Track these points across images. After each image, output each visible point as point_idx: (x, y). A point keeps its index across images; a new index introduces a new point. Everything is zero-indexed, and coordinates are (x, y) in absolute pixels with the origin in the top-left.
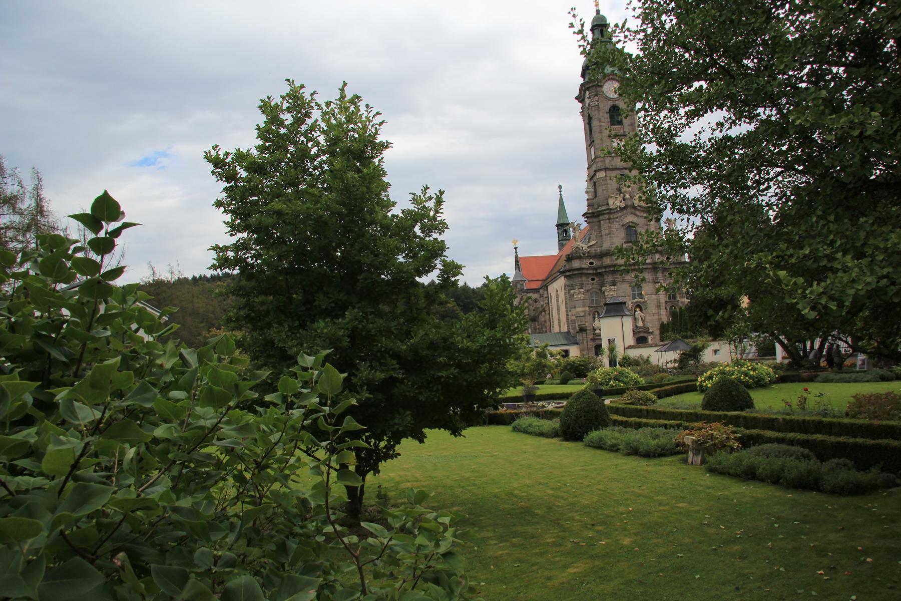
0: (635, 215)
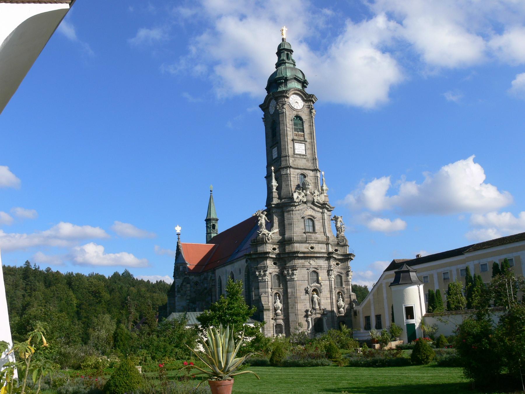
0: (314, 209)
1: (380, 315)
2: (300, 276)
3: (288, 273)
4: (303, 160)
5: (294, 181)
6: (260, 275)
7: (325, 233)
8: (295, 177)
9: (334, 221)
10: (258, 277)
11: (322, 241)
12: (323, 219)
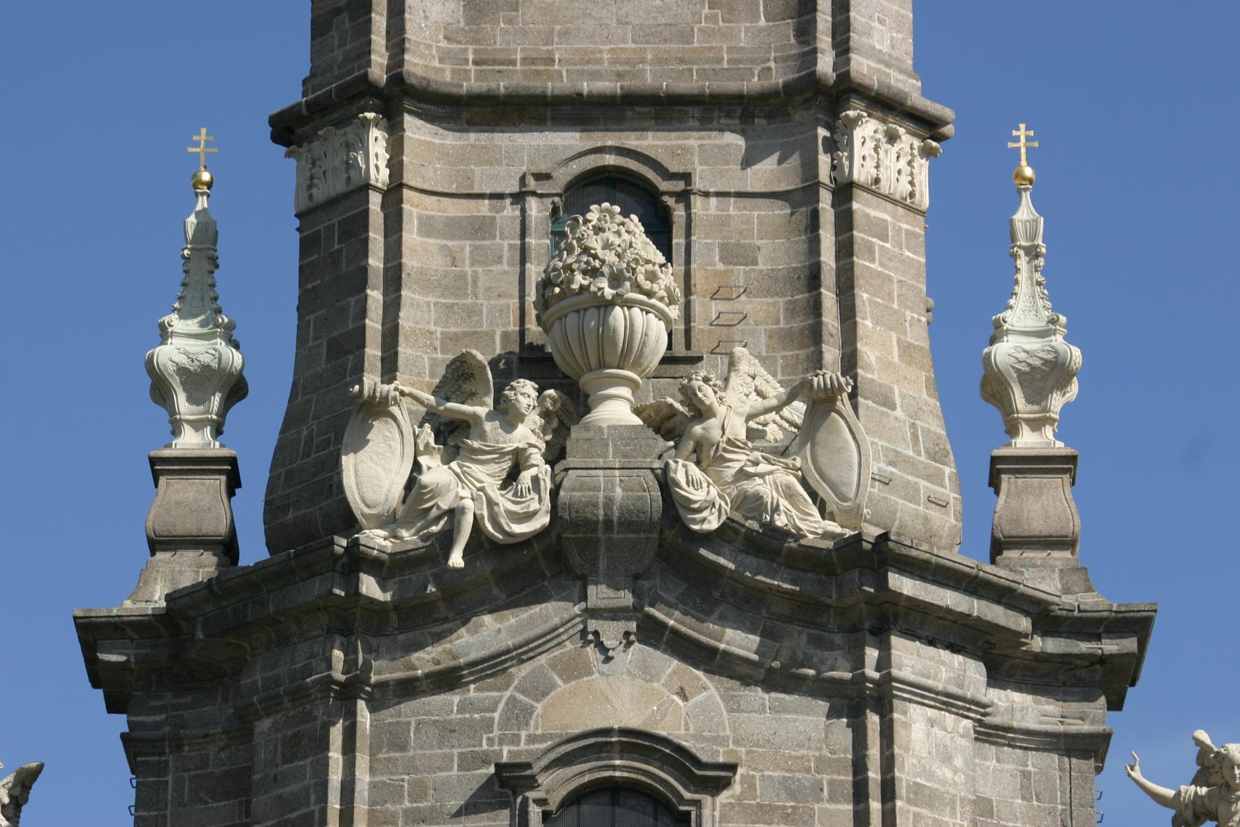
5: (457, 285)
8: (480, 229)
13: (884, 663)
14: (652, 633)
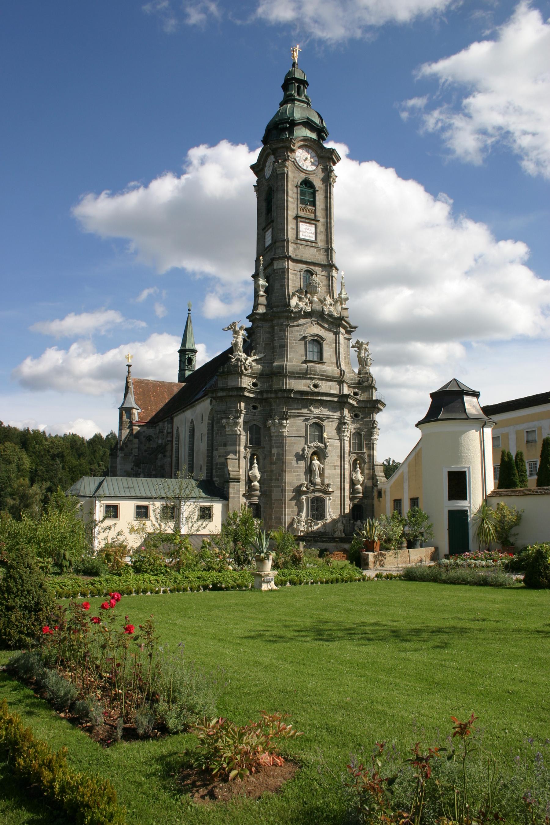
1: (417, 499)
2: (293, 430)
3: (273, 424)
4: (312, 248)
5: (293, 280)
6: (228, 423)
7: (338, 364)
9: (356, 349)
10: (225, 427)
11: (333, 377)
12: (337, 343)
13: (339, 330)
14: (318, 324)
